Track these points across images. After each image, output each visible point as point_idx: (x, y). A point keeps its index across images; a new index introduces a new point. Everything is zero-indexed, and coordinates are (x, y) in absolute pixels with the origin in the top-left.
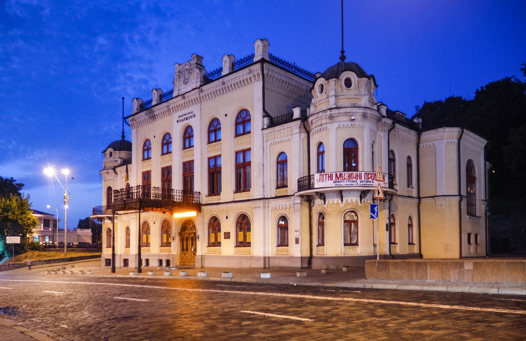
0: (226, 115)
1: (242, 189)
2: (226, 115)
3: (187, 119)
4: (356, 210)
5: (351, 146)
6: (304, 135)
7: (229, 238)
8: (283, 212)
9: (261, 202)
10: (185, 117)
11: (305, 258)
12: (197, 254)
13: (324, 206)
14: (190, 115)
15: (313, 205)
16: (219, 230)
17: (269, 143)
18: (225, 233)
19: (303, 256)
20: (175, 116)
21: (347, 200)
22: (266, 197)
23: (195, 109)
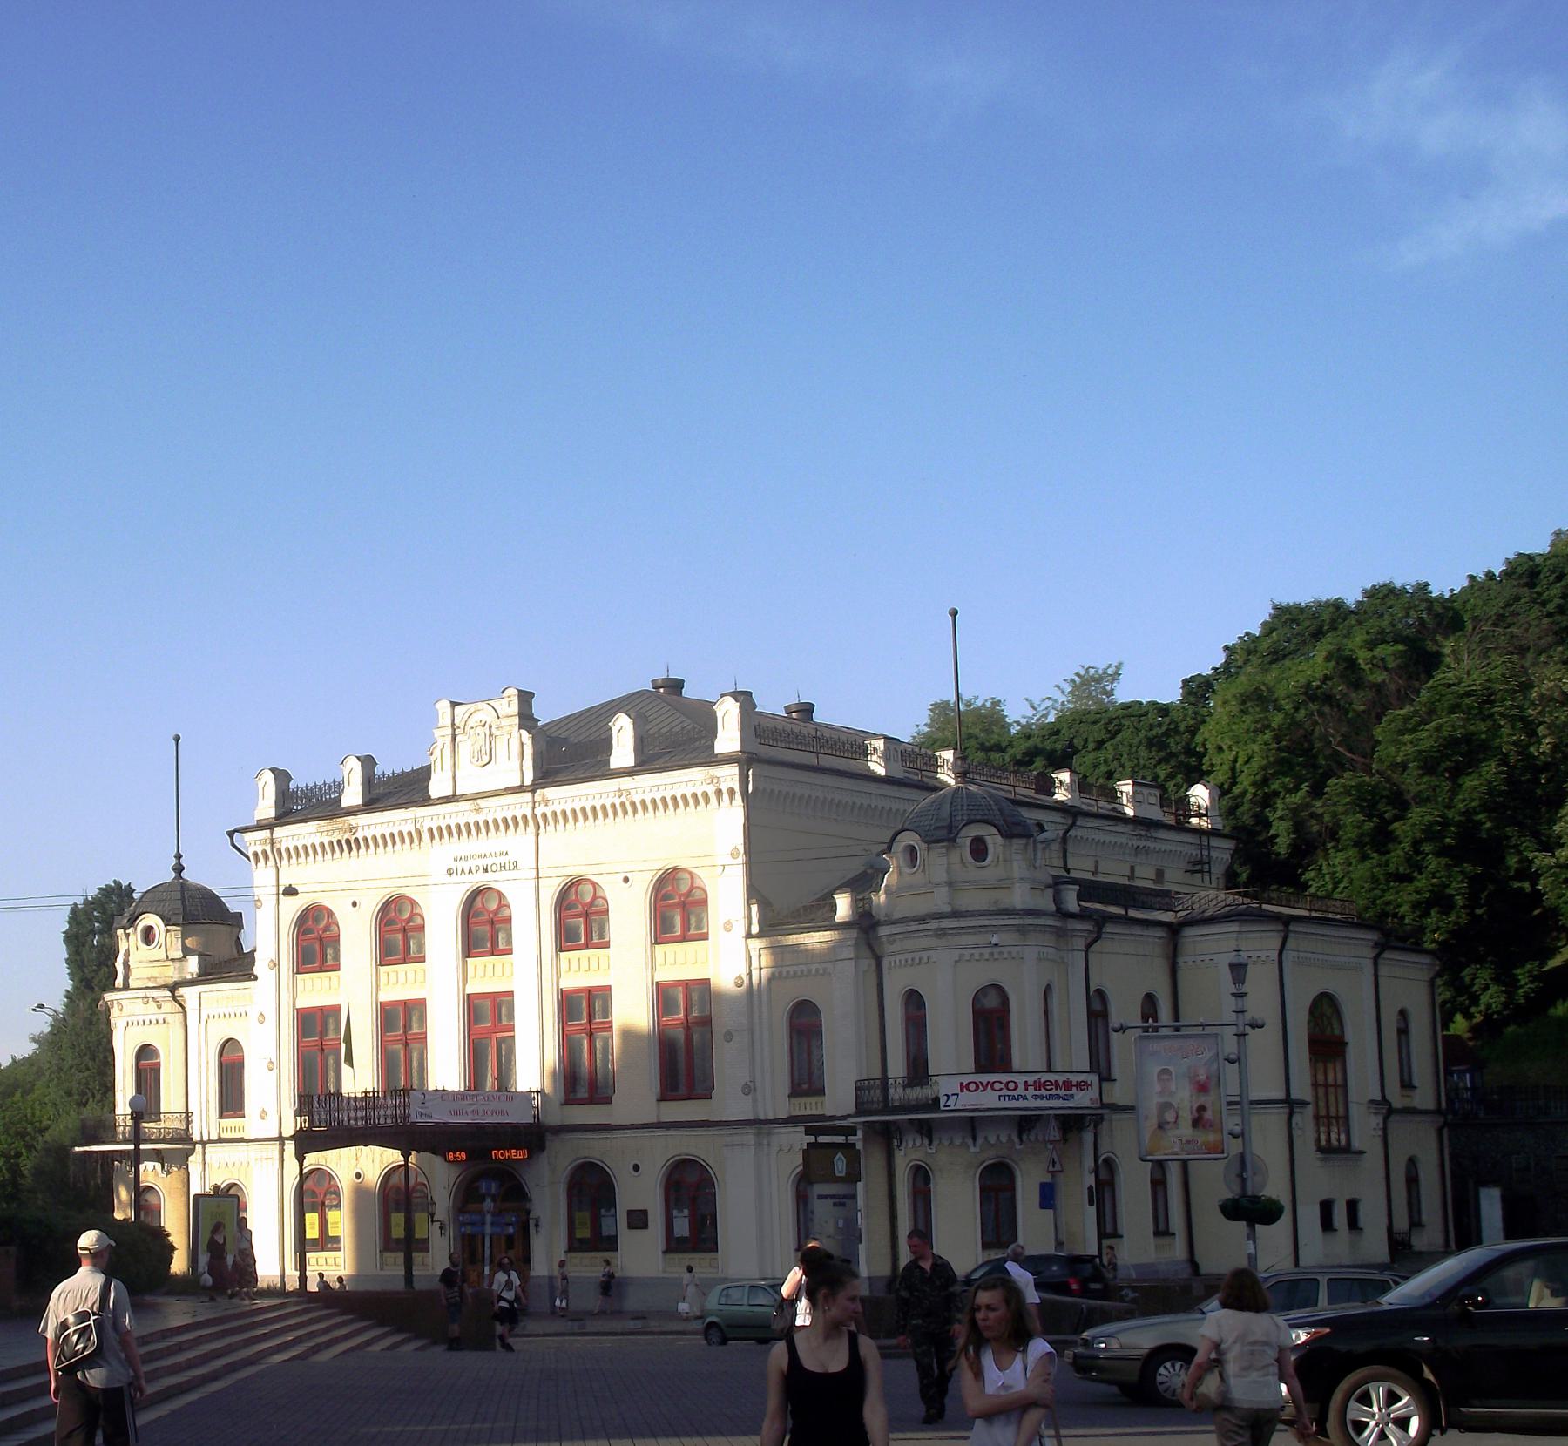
1: (683, 1090)
3: (486, 870)
4: (1007, 1161)
5: (991, 1002)
6: (868, 963)
7: (645, 1226)
9: (750, 1130)
10: (481, 862)
11: (880, 1278)
12: (533, 1273)
13: (930, 1151)
15: (898, 1147)
16: (612, 1204)
18: (630, 1212)
19: (872, 1275)
20: (444, 852)
21: (986, 1138)
22: (762, 1117)
23: (518, 844)
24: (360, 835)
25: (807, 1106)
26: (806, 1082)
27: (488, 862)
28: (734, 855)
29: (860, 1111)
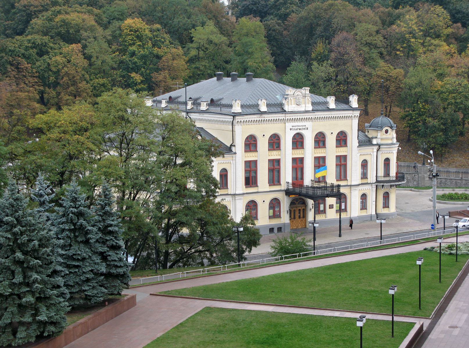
0: (332, 133)
2: (332, 133)
3: (300, 129)
10: (299, 127)
14: (303, 127)
20: (289, 125)
26: (364, 176)
27: (301, 127)
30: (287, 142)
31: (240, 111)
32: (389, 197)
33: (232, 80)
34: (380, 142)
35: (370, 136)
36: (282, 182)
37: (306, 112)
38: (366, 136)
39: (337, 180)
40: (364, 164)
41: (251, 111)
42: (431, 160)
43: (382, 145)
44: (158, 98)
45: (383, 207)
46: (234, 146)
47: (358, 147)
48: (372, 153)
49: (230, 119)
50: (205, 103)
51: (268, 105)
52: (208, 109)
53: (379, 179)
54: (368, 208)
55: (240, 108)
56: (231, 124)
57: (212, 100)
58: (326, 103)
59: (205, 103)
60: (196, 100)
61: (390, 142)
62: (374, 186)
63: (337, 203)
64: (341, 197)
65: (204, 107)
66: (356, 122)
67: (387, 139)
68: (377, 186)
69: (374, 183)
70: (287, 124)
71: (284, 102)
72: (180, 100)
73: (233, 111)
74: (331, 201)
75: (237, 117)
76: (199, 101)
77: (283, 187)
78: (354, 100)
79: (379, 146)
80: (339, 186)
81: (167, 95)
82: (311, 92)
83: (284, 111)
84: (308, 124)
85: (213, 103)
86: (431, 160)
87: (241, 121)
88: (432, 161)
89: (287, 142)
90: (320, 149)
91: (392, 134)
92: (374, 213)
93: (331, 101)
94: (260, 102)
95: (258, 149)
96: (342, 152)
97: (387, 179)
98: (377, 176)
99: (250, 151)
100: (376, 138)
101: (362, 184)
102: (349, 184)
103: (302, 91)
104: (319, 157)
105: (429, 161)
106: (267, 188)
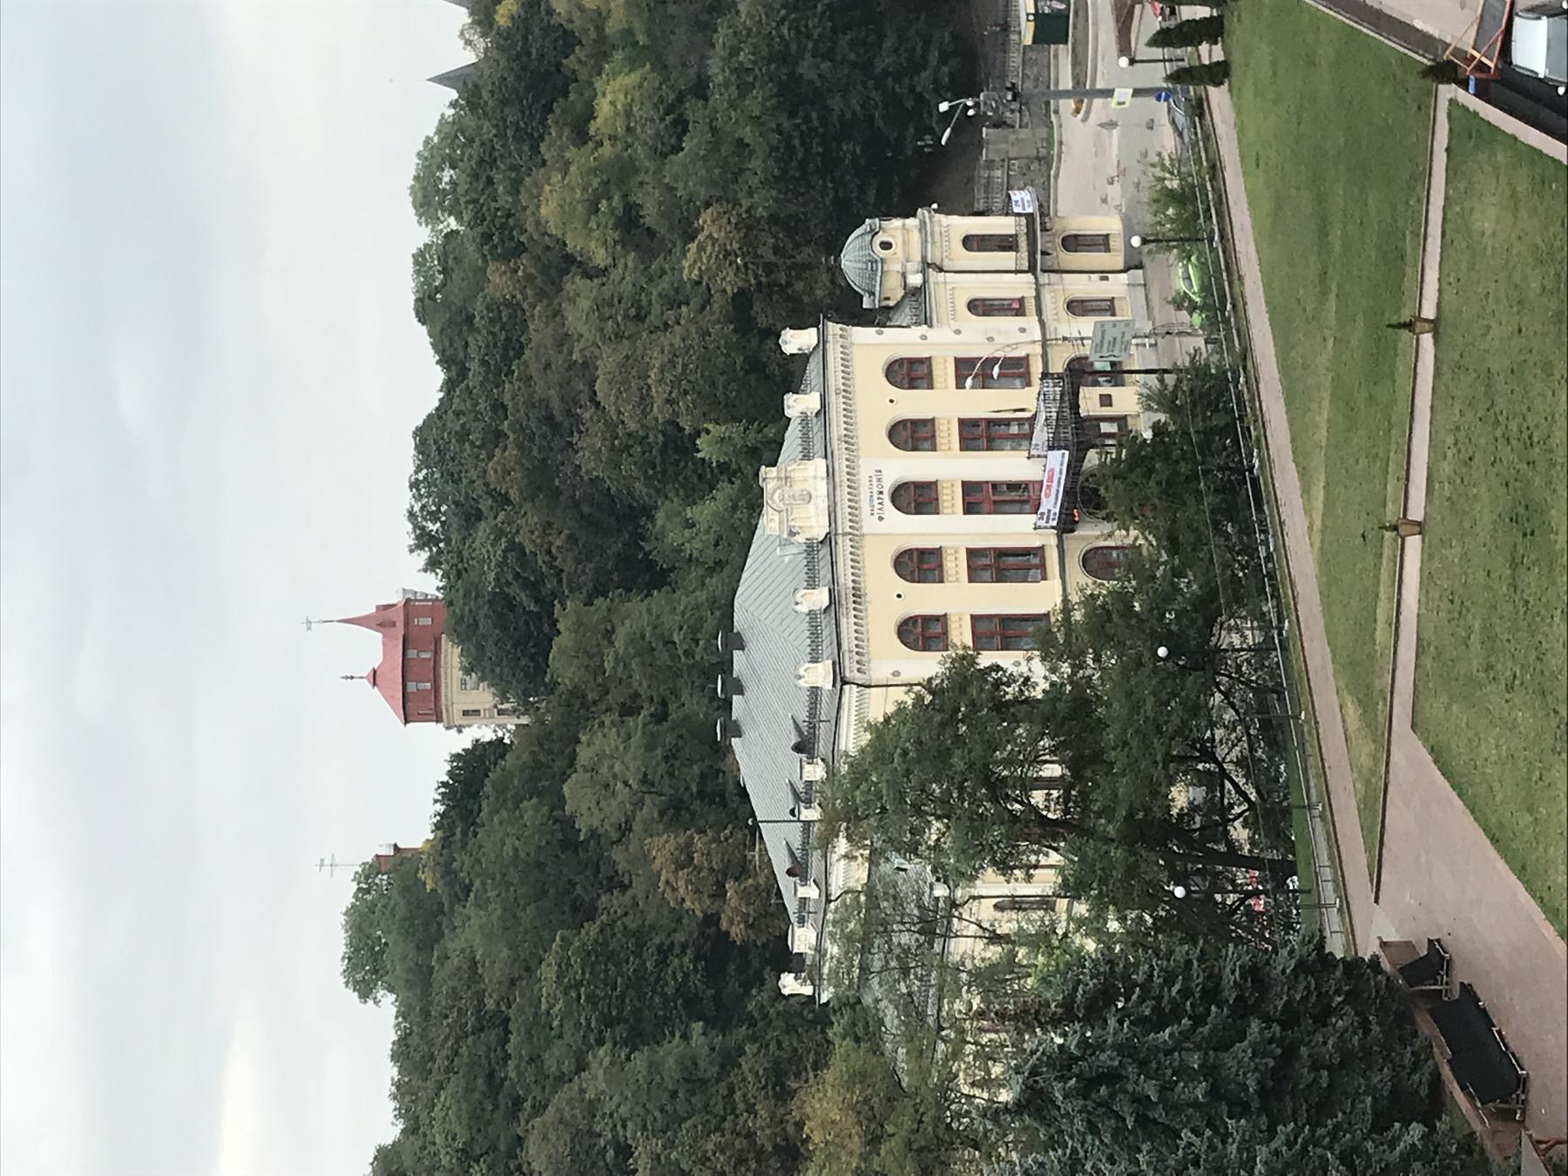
0: (892, 401)
2: (892, 401)
3: (881, 493)
8: (1062, 306)
14: (875, 483)
17: (951, 322)
20: (869, 524)
24: (852, 585)
25: (1031, 306)
26: (1015, 308)
27: (875, 490)
28: (881, 333)
29: (1034, 274)
30: (918, 530)
31: (830, 662)
32: (1076, 236)
33: (741, 692)
34: (914, 265)
35: (900, 293)
36: (1035, 543)
37: (831, 473)
38: (898, 305)
39: (1029, 384)
40: (980, 307)
41: (827, 633)
42: (967, 108)
43: (924, 258)
44: (792, 906)
45: (1108, 250)
46: (930, 680)
47: (931, 326)
48: (949, 287)
49: (851, 693)
50: (807, 768)
51: (812, 584)
52: (823, 760)
53: (1025, 266)
54: (1109, 296)
55: (819, 665)
56: (867, 690)
57: (798, 748)
58: (805, 418)
59: (807, 768)
60: (796, 796)
61: (916, 236)
62: (1044, 278)
63: (1096, 384)
64: (1079, 373)
65: (816, 772)
66: (862, 335)
67: (905, 243)
68: (1044, 271)
69: (1036, 278)
70: (864, 530)
71: (800, 539)
72: (796, 844)
73: (829, 686)
74: (1089, 401)
75: (847, 674)
76: (800, 787)
77: (1049, 540)
78: (795, 341)
79: (929, 265)
80: (1045, 375)
81: (785, 883)
82: (773, 463)
83: (829, 540)
84: (865, 471)
85: (805, 747)
86: (967, 108)
87: (858, 662)
88: (970, 103)
89: (918, 530)
90: (935, 373)
91: (895, 228)
92: (1123, 277)
93: (798, 405)
94: (803, 608)
95: (931, 479)
96: (944, 372)
97: (1023, 243)
98: (1016, 272)
99: (930, 374)
100: (904, 275)
101: (1039, 312)
102: (1038, 349)
103: (769, 487)
104: (962, 438)
105: (971, 112)
106: (1054, 583)
